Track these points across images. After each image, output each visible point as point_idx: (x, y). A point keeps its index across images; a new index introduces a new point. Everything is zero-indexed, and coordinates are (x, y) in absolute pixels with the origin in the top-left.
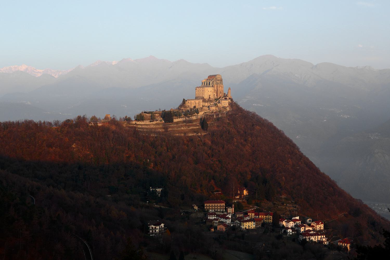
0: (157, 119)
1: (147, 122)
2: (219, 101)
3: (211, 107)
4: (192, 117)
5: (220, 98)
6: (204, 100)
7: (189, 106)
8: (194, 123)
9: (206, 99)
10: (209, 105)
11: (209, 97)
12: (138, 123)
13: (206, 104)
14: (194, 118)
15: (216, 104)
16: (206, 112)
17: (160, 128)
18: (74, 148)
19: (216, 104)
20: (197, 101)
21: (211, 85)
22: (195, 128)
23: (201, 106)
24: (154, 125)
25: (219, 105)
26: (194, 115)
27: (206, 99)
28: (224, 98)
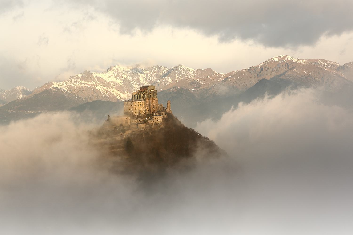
2: (151, 117)
3: (140, 124)
5: (153, 113)
6: (133, 117)
9: (135, 116)
10: (139, 122)
11: (140, 113)
13: (135, 121)
16: (134, 130)
19: (146, 121)
21: (142, 99)
23: (129, 124)
25: (150, 121)
26: (120, 134)
27: (135, 116)
28: (157, 114)
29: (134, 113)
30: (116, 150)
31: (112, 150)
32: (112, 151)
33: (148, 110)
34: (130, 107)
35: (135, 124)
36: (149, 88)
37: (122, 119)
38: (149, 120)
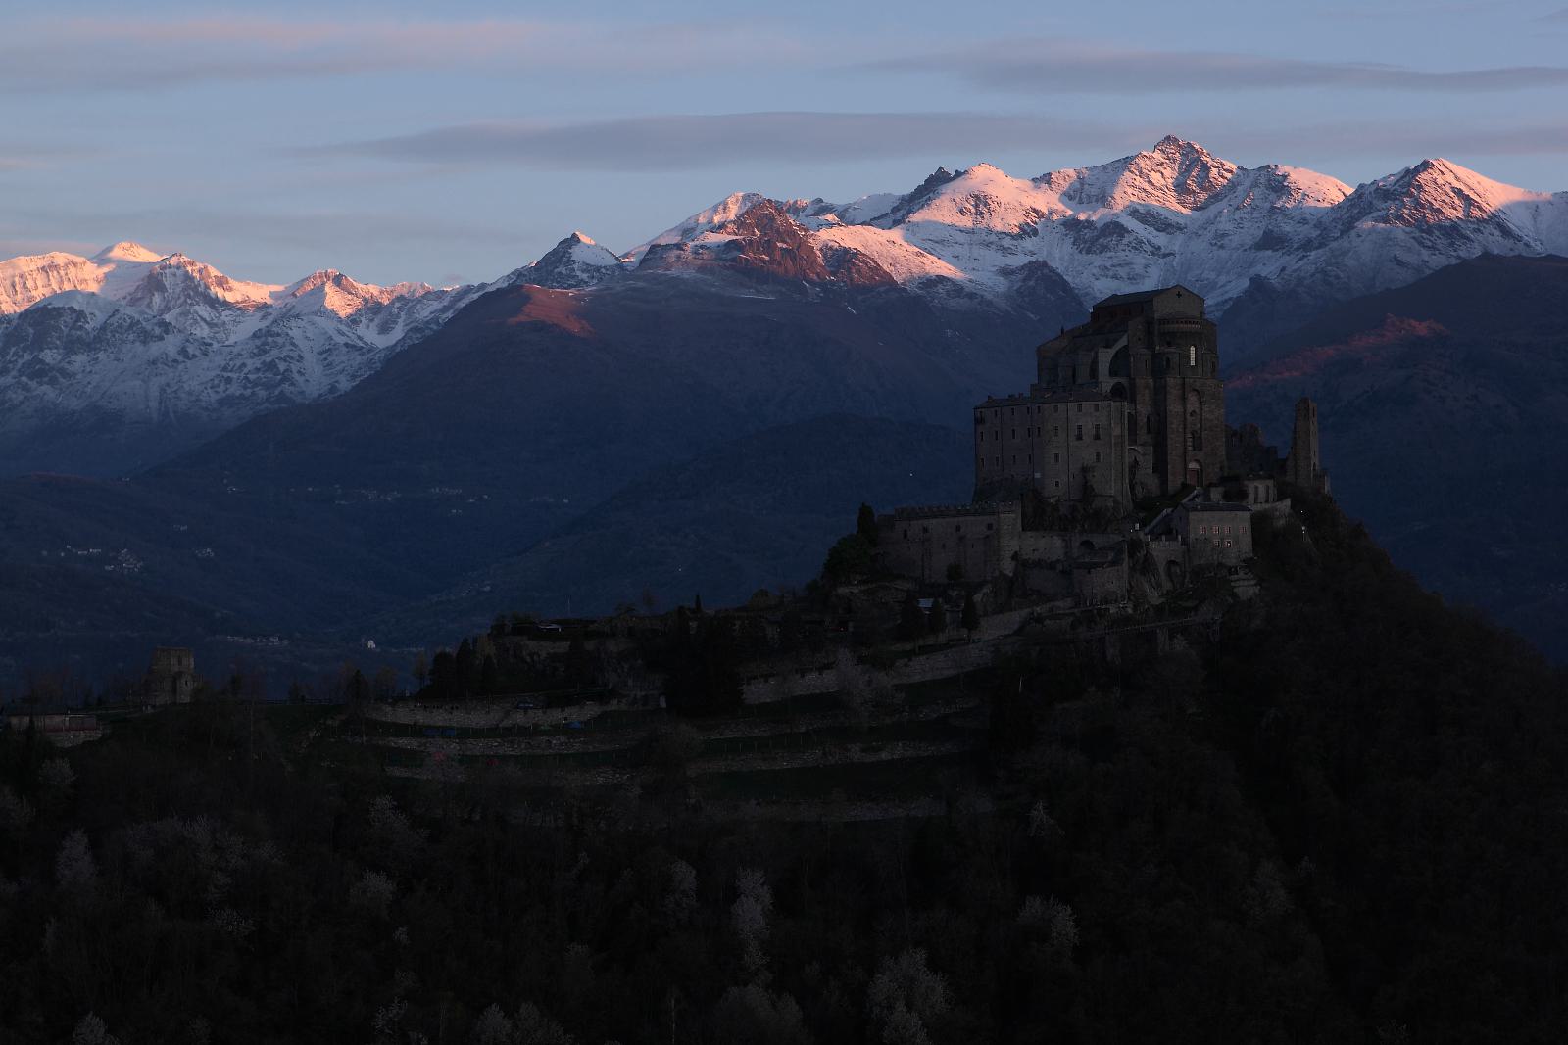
3: (1090, 567)
5: (1185, 488)
6: (1039, 515)
11: (1087, 491)
12: (439, 717)
14: (924, 669)
15: (1135, 546)
23: (1008, 567)
26: (942, 638)
28: (1216, 494)
32: (884, 756)
35: (1052, 566)
36: (1161, 309)
37: (958, 528)
38: (1156, 537)
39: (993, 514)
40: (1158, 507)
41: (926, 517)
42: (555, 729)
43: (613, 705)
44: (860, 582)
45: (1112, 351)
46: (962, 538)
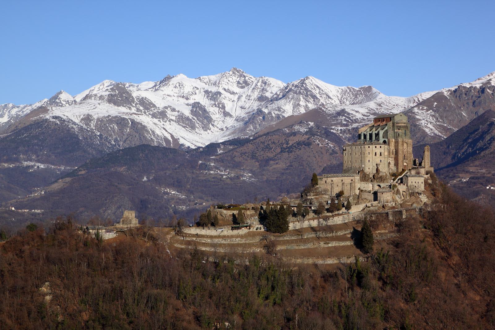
0: (249, 221)
1: (227, 231)
4: (336, 218)
5: (403, 170)
6: (365, 178)
7: (326, 191)
8: (340, 233)
10: (376, 188)
11: (377, 170)
13: (369, 186)
14: (338, 220)
16: (369, 205)
17: (256, 246)
18: (45, 295)
20: (347, 180)
21: (381, 140)
22: (342, 244)
23: (357, 192)
24: (242, 237)
26: (340, 212)
27: (369, 175)
29: (367, 170)
30: (337, 245)
31: (329, 243)
32: (330, 245)
33: (392, 163)
34: (357, 156)
35: (370, 192)
36: (397, 119)
37: (342, 181)
39: (353, 177)
40: (399, 176)
41: (332, 177)
42: (237, 236)
43: (251, 230)
44: (313, 195)
45: (383, 131)
46: (343, 184)
